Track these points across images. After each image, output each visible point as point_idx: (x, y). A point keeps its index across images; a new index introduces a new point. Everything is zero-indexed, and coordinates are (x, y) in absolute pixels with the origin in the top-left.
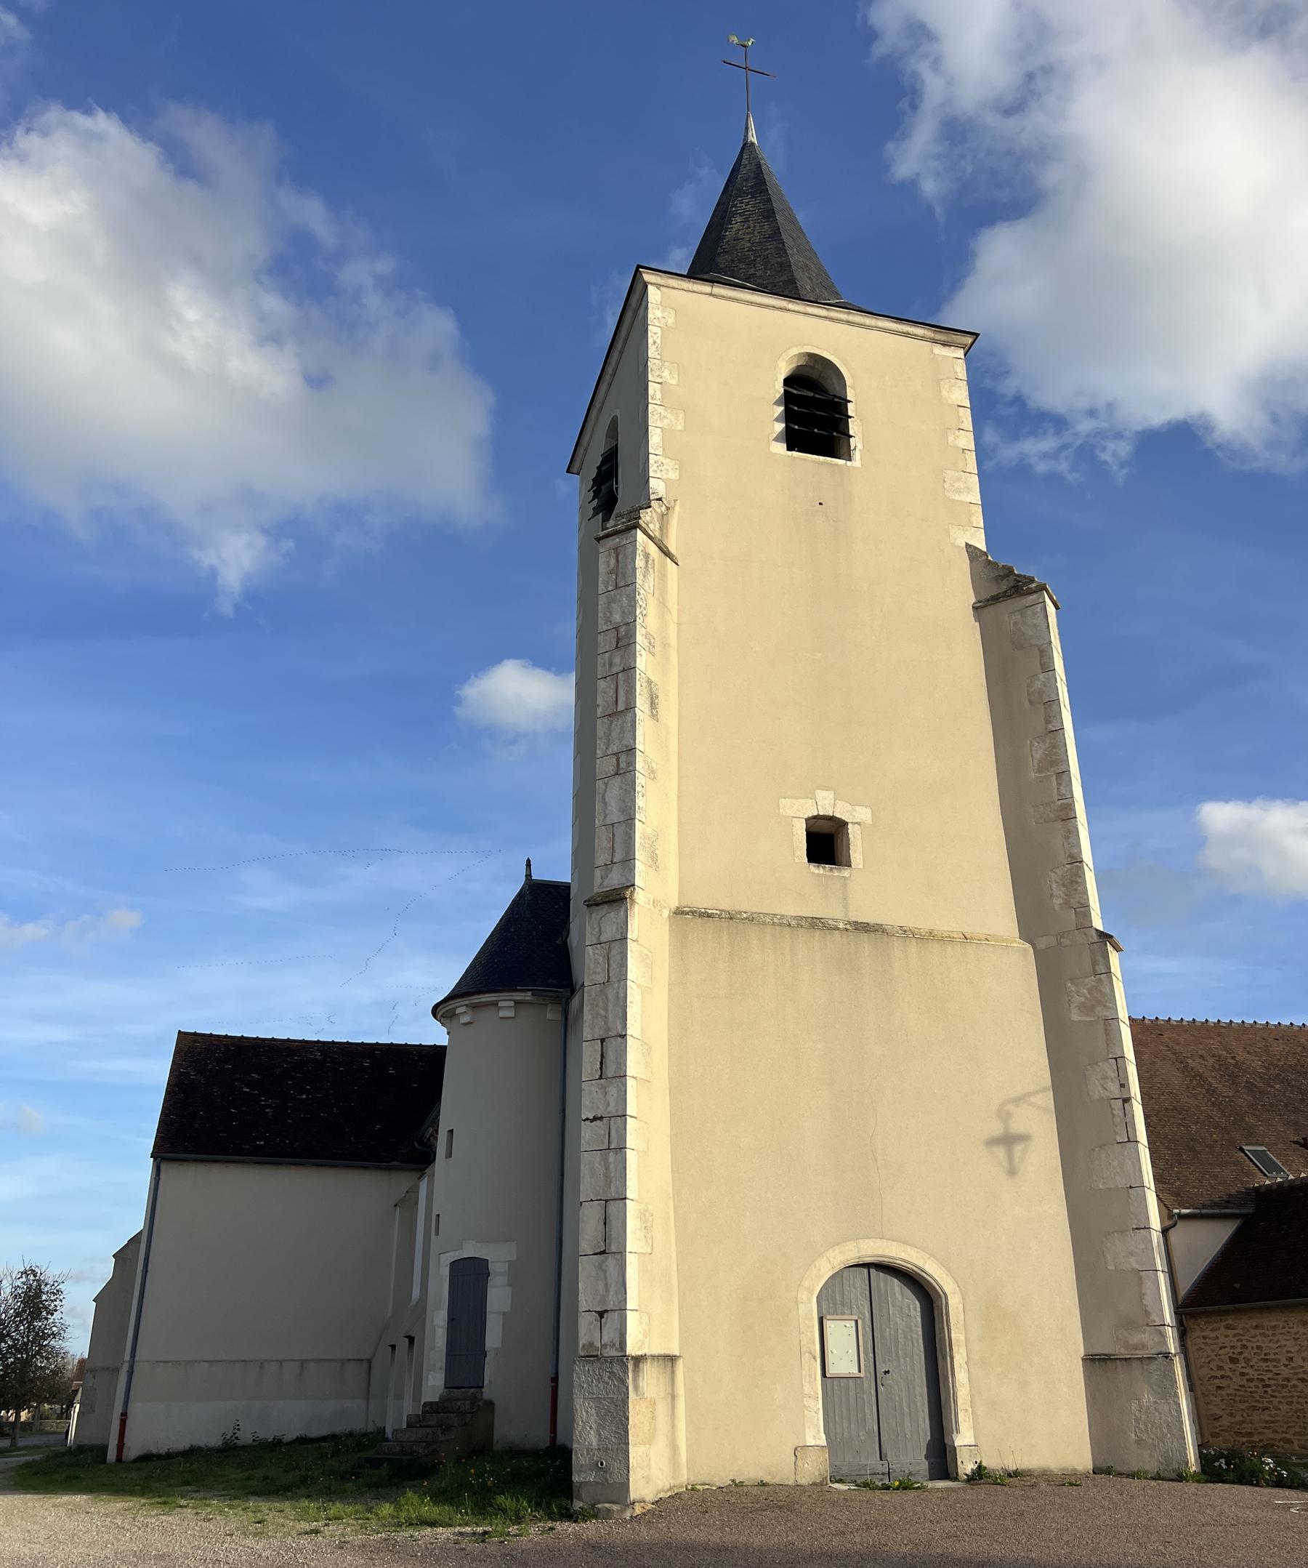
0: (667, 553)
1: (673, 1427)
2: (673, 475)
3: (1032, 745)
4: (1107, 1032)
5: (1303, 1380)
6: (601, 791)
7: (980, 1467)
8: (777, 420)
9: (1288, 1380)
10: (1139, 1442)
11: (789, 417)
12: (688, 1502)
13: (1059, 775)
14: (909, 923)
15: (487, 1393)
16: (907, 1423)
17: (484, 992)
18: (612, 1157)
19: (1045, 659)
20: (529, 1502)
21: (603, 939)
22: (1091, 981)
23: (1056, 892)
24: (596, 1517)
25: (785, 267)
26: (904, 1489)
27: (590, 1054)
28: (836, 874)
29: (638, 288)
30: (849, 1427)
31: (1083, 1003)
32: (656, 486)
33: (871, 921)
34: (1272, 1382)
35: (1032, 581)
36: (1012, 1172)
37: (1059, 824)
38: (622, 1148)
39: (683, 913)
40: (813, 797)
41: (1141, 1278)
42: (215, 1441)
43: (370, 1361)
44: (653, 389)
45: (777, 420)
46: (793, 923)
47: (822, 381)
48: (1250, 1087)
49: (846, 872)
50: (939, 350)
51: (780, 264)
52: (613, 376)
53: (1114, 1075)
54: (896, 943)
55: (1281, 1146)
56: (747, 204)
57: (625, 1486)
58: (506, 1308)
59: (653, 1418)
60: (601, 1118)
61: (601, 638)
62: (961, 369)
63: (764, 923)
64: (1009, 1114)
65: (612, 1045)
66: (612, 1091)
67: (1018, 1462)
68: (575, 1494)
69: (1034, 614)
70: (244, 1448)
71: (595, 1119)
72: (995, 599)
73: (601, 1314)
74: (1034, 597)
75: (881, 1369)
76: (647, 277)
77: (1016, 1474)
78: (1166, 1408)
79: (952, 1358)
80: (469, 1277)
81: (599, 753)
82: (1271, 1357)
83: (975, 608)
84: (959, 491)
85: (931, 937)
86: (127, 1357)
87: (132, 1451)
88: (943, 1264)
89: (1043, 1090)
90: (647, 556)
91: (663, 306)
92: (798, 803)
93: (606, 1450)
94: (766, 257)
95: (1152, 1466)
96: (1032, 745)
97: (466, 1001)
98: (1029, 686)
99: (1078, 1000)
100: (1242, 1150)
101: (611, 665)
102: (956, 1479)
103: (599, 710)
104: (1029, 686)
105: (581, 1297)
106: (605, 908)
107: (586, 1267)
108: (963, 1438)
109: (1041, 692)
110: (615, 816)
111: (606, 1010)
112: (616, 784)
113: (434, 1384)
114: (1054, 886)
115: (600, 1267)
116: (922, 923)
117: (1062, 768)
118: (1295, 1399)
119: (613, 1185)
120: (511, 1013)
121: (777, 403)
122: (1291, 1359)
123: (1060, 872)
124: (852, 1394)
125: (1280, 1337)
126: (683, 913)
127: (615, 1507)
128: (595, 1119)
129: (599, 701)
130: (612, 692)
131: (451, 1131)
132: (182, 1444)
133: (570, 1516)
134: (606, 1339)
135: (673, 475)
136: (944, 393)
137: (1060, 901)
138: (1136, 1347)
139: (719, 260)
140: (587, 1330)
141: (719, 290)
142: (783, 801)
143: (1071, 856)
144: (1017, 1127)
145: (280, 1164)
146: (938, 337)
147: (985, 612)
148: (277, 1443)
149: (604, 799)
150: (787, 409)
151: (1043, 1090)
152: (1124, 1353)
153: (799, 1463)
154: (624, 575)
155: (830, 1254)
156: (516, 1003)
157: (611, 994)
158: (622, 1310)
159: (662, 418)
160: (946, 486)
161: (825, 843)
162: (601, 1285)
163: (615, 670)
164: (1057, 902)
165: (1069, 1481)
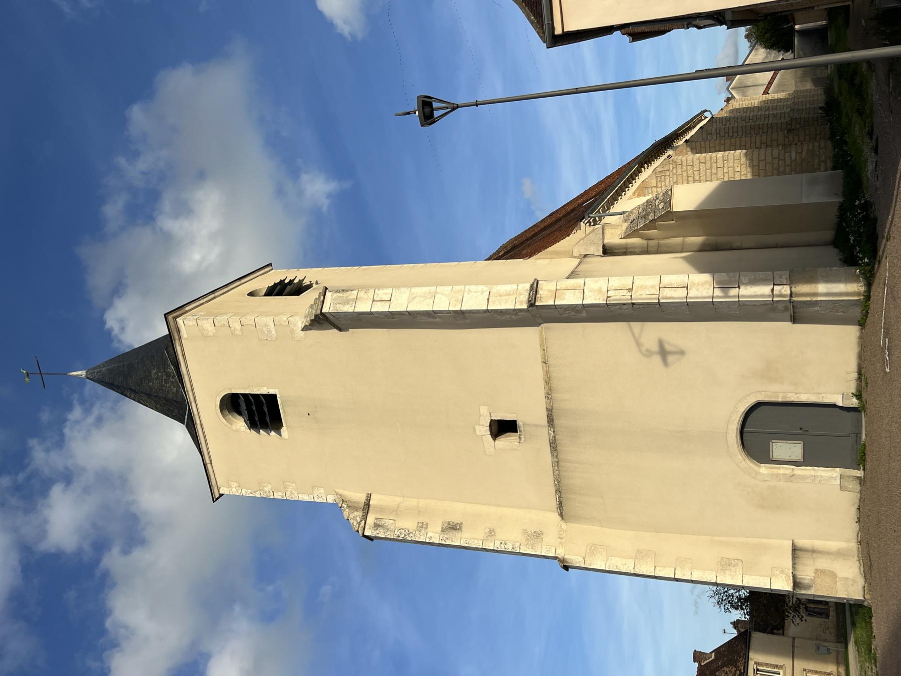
64: (648, 350)
77: (860, 373)
85: (548, 381)
121: (259, 433)
144: (655, 348)
146: (177, 337)
161: (503, 428)
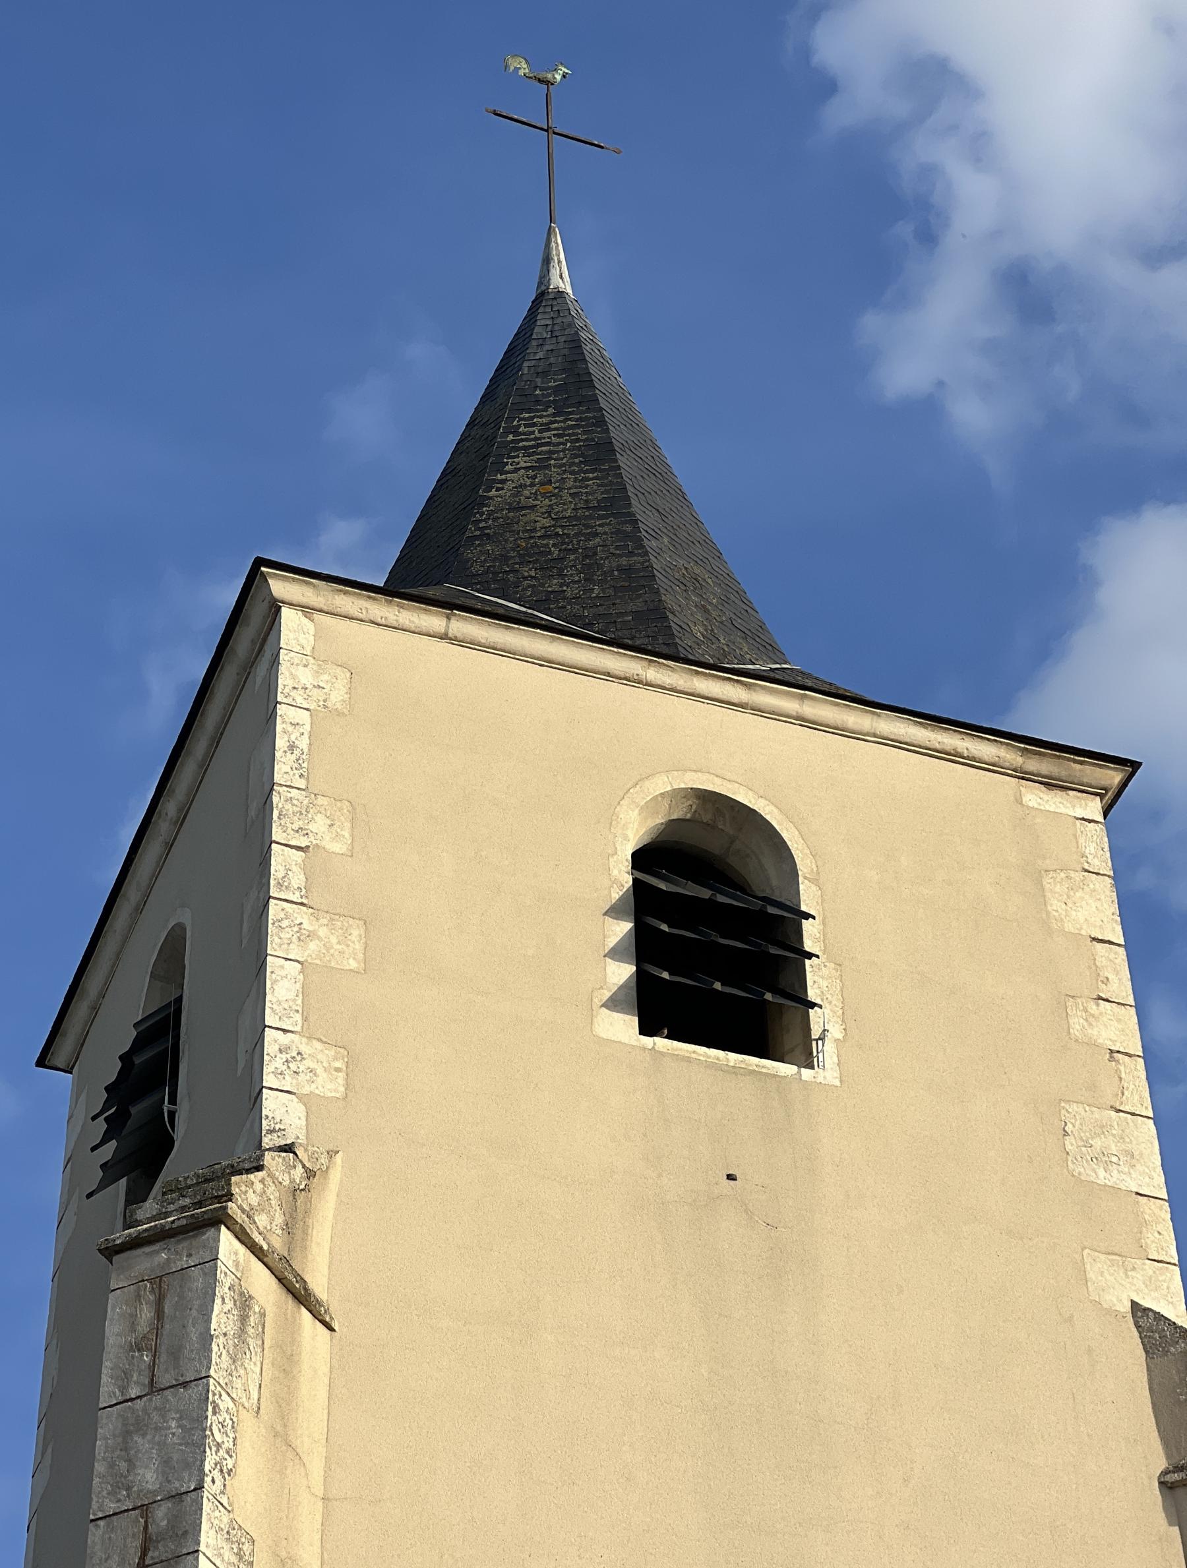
2: (330, 1086)
8: (615, 954)
11: (645, 947)
25: (639, 577)
29: (256, 612)
32: (281, 1112)
44: (281, 861)
45: (615, 954)
47: (733, 861)
50: (1035, 797)
51: (627, 571)
52: (181, 821)
56: (545, 428)
61: (96, 1534)
62: (1095, 845)
76: (280, 587)
84: (1103, 1159)
90: (244, 1302)
91: (318, 658)
121: (614, 912)
135: (330, 1086)
136: (1055, 905)
141: (465, 626)
146: (1033, 764)
154: (175, 1355)
159: (304, 937)
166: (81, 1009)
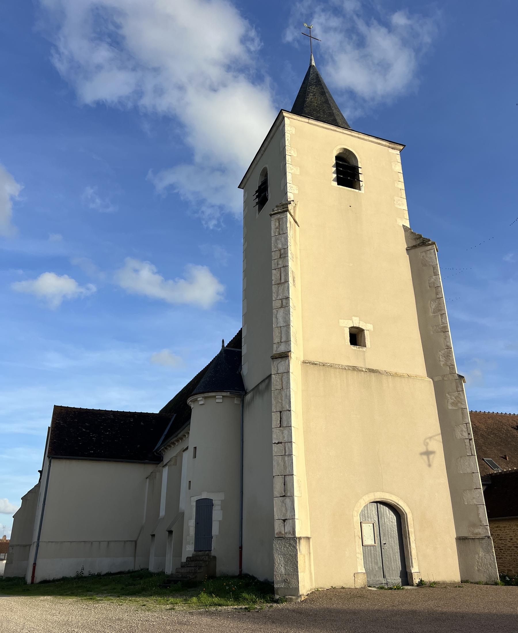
0: (296, 222)
1: (310, 565)
2: (296, 192)
3: (431, 303)
4: (463, 413)
5: (516, 547)
6: (275, 314)
7: (421, 580)
8: (334, 173)
9: (510, 547)
10: (479, 570)
11: (338, 172)
12: (316, 595)
13: (442, 315)
14: (388, 370)
15: (213, 553)
16: (393, 564)
17: (210, 392)
18: (286, 458)
19: (435, 271)
20: (255, 596)
21: (279, 372)
22: (456, 394)
23: (441, 359)
24: (286, 601)
25: (332, 114)
26: (398, 589)
27: (275, 417)
28: (361, 349)
29: (280, 118)
30: (372, 565)
31: (453, 402)
32: (290, 196)
33: (374, 369)
34: (503, 548)
35: (429, 241)
36: (430, 465)
37: (442, 334)
38: (290, 455)
39: (306, 363)
40: (351, 319)
41: (478, 508)
42: (73, 574)
43: (136, 542)
44: (288, 157)
45: (334, 173)
46: (347, 368)
47: (348, 159)
48: (482, 436)
49: (364, 349)
50: (391, 150)
51: (330, 113)
52: (265, 151)
53: (465, 430)
54: (384, 377)
55: (497, 458)
56: (314, 89)
57: (297, 589)
58: (221, 519)
59: (305, 562)
60: (281, 443)
61: (273, 253)
62: (399, 158)
63: (336, 368)
64: (428, 443)
65: (284, 414)
66: (286, 432)
67: (435, 578)
68: (276, 592)
69: (431, 253)
70: (85, 577)
71: (278, 443)
72: (415, 247)
73: (284, 521)
74: (430, 247)
75: (383, 542)
76: (285, 114)
77: (435, 583)
78: (489, 557)
79: (409, 538)
80: (204, 507)
81: (274, 299)
82: (504, 538)
83: (407, 250)
84: (399, 205)
85: (396, 375)
86: (35, 539)
87: (38, 579)
88: (405, 502)
89: (438, 435)
90: (290, 222)
91: (290, 125)
92: (346, 321)
93: (289, 575)
94: (324, 110)
95: (484, 579)
96: (431, 303)
97: (202, 395)
98: (429, 280)
99: (451, 401)
100: (483, 460)
101: (278, 264)
102: (413, 585)
103: (273, 282)
104: (429, 280)
105: (275, 513)
106: (280, 360)
107: (277, 502)
108: (414, 570)
109: (434, 283)
110: (281, 324)
111: (282, 400)
112: (281, 311)
113: (189, 549)
114: (441, 357)
115: (283, 502)
116: (393, 370)
117: (443, 312)
118: (513, 555)
119: (287, 469)
120: (221, 401)
121: (333, 166)
122: (512, 539)
123: (443, 352)
124: (372, 552)
125: (507, 531)
126: (306, 363)
127: (294, 597)
128: (278, 443)
129: (273, 278)
130: (279, 275)
131: (195, 448)
132: (59, 576)
133: (277, 602)
134: (286, 530)
135: (296, 192)
136: (393, 167)
137: (443, 363)
138: (477, 534)
139: (305, 109)
140: (278, 527)
141: (311, 121)
142: (340, 321)
143: (447, 346)
144: (430, 449)
145: (110, 461)
146: (391, 145)
147: (413, 251)
148: (99, 575)
149: (276, 317)
150: (337, 169)
151: (438, 435)
152: (472, 536)
153: (356, 579)
154: (282, 229)
155: (364, 497)
156: (223, 396)
157: (283, 394)
158: (293, 519)
159: (291, 169)
160: (395, 202)
161: (356, 337)
162: (284, 509)
163: (279, 266)
164: (442, 363)
165: (454, 585)
166: (246, 179)
